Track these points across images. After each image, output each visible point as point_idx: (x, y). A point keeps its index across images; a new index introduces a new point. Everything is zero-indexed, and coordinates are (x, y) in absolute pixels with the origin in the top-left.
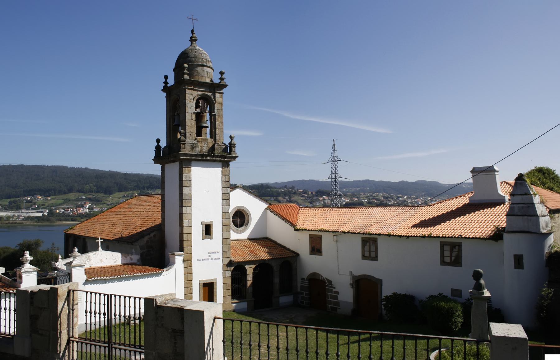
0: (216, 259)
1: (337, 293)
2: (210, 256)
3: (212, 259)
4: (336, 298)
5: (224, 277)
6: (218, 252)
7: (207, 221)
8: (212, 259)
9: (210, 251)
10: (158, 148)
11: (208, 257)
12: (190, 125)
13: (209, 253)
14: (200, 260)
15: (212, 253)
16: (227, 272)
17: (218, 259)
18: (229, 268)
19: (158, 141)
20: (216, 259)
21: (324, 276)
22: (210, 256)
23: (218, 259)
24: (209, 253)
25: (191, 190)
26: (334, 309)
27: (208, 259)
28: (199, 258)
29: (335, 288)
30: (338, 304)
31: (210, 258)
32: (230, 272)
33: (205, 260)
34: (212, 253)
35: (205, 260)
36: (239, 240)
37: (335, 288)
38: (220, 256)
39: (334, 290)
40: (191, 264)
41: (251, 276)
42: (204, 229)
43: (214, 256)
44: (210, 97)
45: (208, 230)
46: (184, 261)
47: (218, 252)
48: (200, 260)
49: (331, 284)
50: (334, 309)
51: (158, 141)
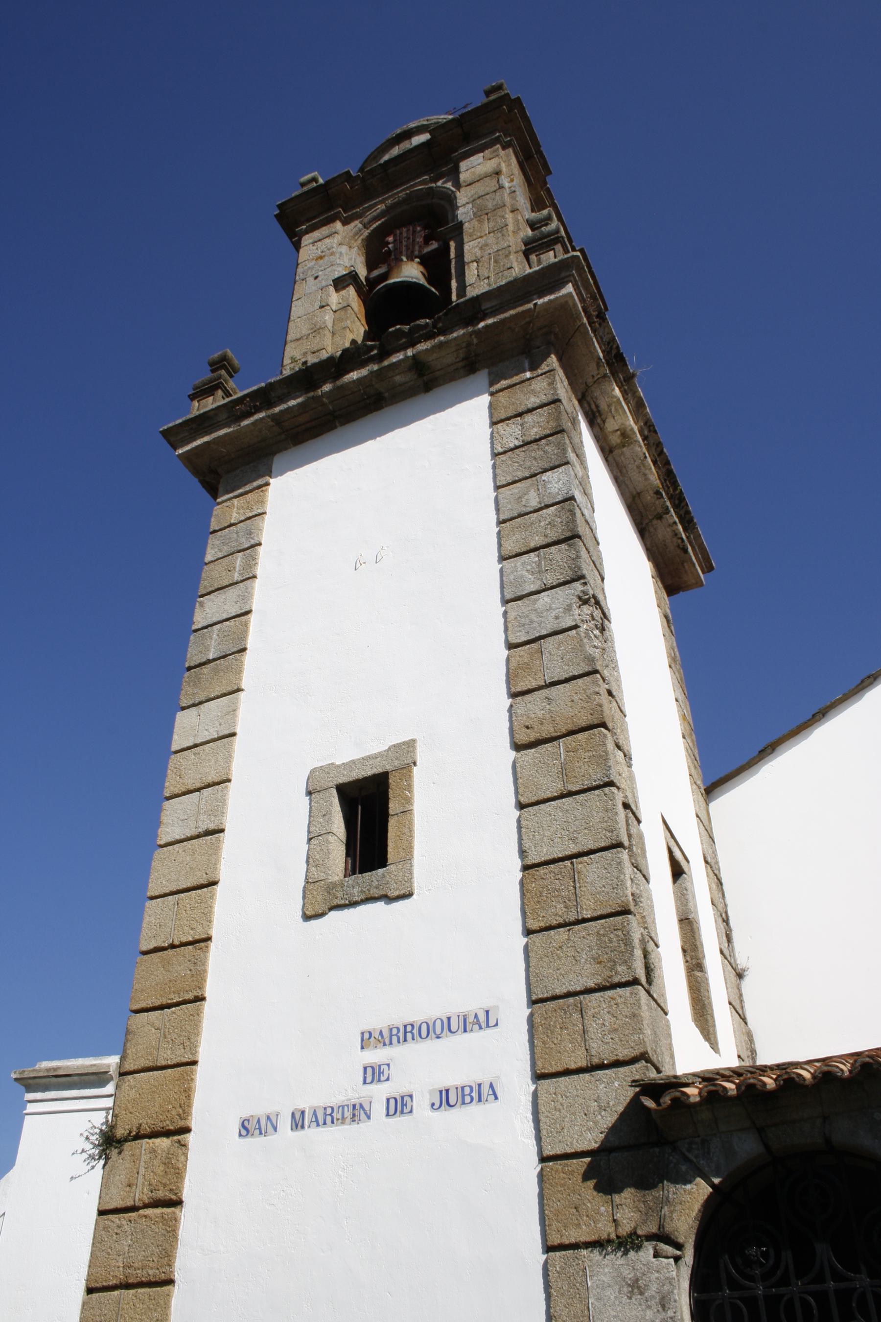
0: (444, 1099)
3: (399, 1106)
7: (354, 749)
8: (399, 1106)
9: (378, 1022)
11: (347, 1087)
13: (367, 1040)
15: (406, 1033)
18: (627, 1210)
20: (444, 1099)
22: (374, 1074)
24: (367, 1040)
27: (357, 1112)
28: (259, 1110)
31: (379, 1093)
33: (329, 1116)
34: (406, 1033)
35: (329, 1116)
38: (505, 1052)
40: (175, 1171)
43: (420, 1068)
46: (110, 1142)
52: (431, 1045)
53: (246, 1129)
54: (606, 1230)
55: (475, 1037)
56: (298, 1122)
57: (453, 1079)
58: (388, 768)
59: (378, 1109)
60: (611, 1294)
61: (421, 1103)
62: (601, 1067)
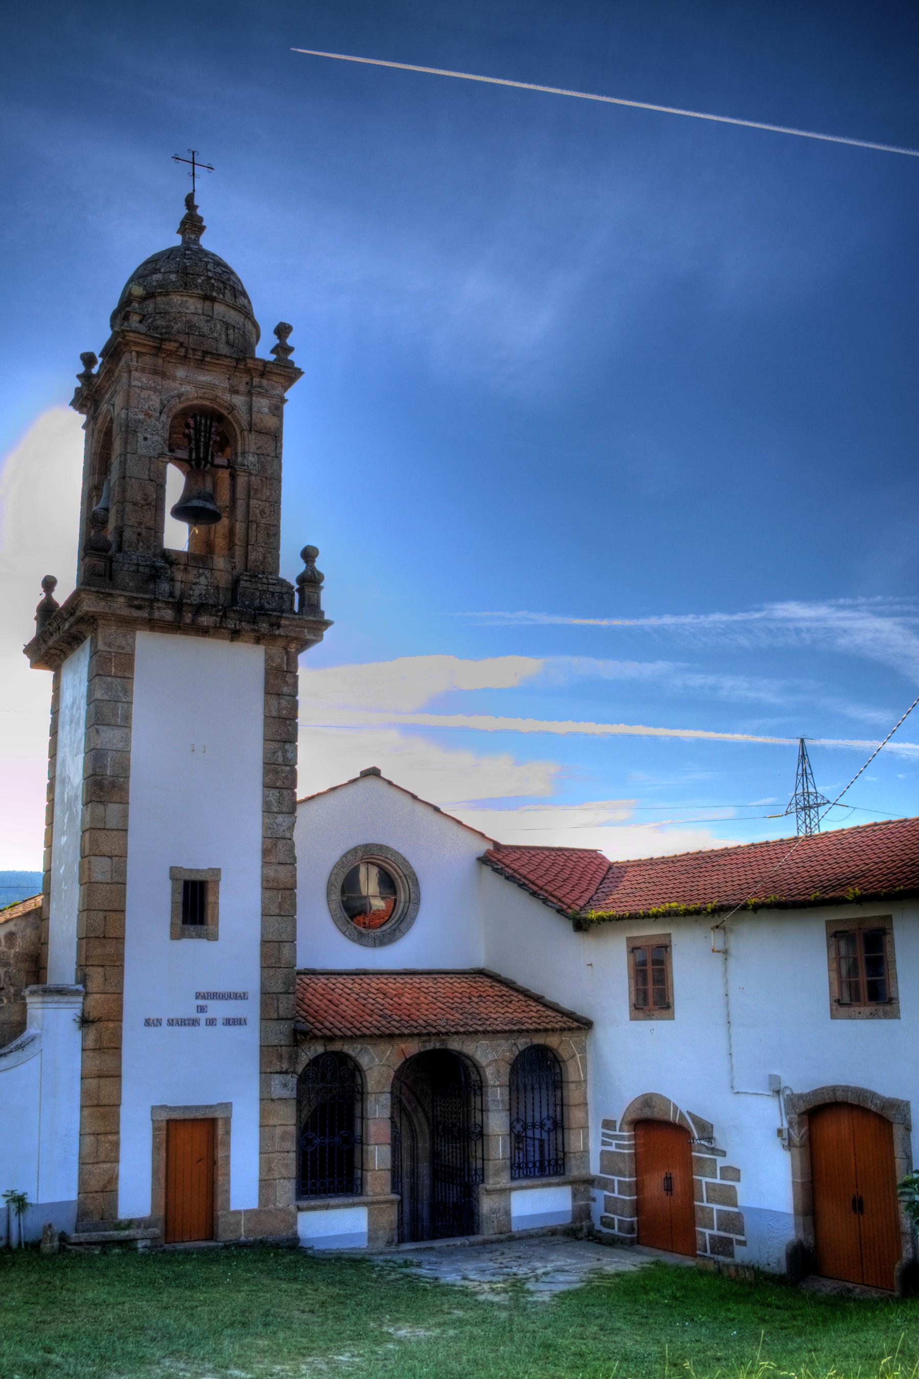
0: (228, 1022)
1: (733, 1173)
2: (201, 1009)
3: (211, 1022)
4: (728, 1196)
5: (266, 1100)
6: (242, 996)
8: (211, 1022)
9: (204, 989)
10: (47, 611)
12: (139, 498)
14: (158, 1022)
16: (277, 1080)
17: (239, 1022)
19: (49, 584)
20: (228, 1022)
21: (683, 1108)
22: (201, 1009)
23: (239, 1022)
24: (199, 996)
25: (127, 740)
26: (723, 1246)
27: (194, 1022)
28: (153, 1016)
29: (723, 1154)
30: (733, 1222)
31: (203, 1017)
32: (293, 1081)
33: (183, 1022)
35: (183, 1022)
36: (366, 973)
37: (723, 1154)
38: (251, 1009)
39: (721, 1162)
41: (386, 1099)
42: (180, 899)
43: (218, 1009)
44: (232, 408)
45: (194, 903)
46: (85, 1022)
47: (242, 996)
48: (158, 1022)
49: (710, 1139)
50: (723, 1246)
51: (49, 584)
52: (223, 1002)
53: (148, 1023)
54: (278, 1068)
55: (240, 1002)
56: (171, 1023)
57: (231, 1015)
58: (208, 879)
59: (203, 1022)
60: (278, 1087)
61: (219, 1022)
62: (282, 1019)
